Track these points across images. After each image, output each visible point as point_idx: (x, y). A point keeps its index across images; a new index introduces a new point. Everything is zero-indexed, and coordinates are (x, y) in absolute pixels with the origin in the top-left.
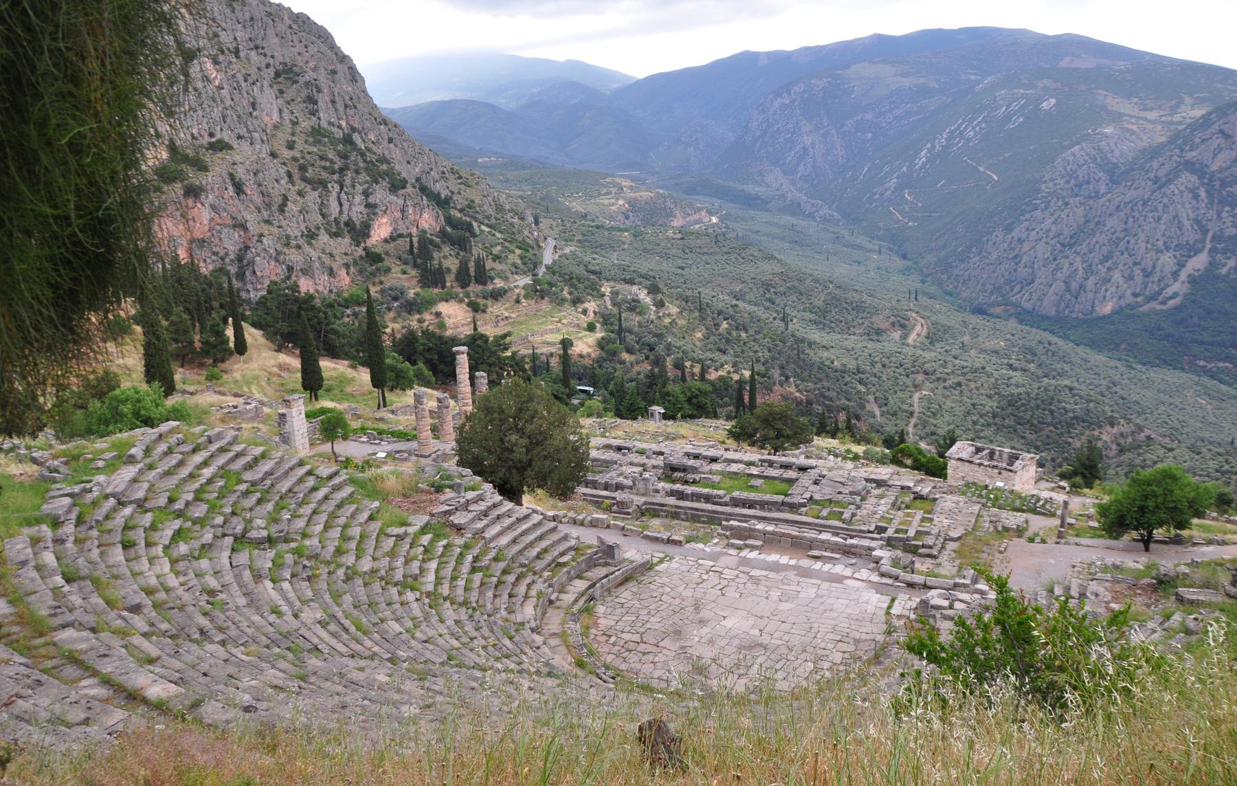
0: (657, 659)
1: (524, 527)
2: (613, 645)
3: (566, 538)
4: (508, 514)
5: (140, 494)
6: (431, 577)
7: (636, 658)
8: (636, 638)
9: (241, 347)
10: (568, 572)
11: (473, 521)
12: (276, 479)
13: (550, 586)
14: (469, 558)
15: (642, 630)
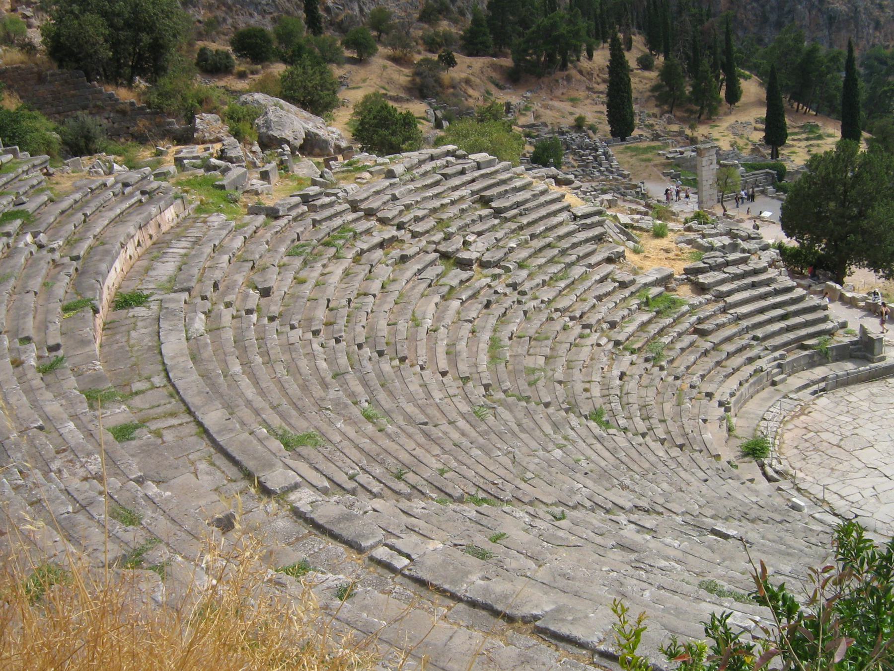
0: (839, 467)
1: (779, 299)
2: (806, 441)
3: (825, 319)
4: (768, 282)
5: (375, 205)
6: (631, 328)
7: (818, 460)
8: (835, 440)
9: (733, 96)
10: (810, 357)
11: (722, 282)
12: (527, 209)
13: (779, 366)
14: (694, 319)
15: (848, 434)
